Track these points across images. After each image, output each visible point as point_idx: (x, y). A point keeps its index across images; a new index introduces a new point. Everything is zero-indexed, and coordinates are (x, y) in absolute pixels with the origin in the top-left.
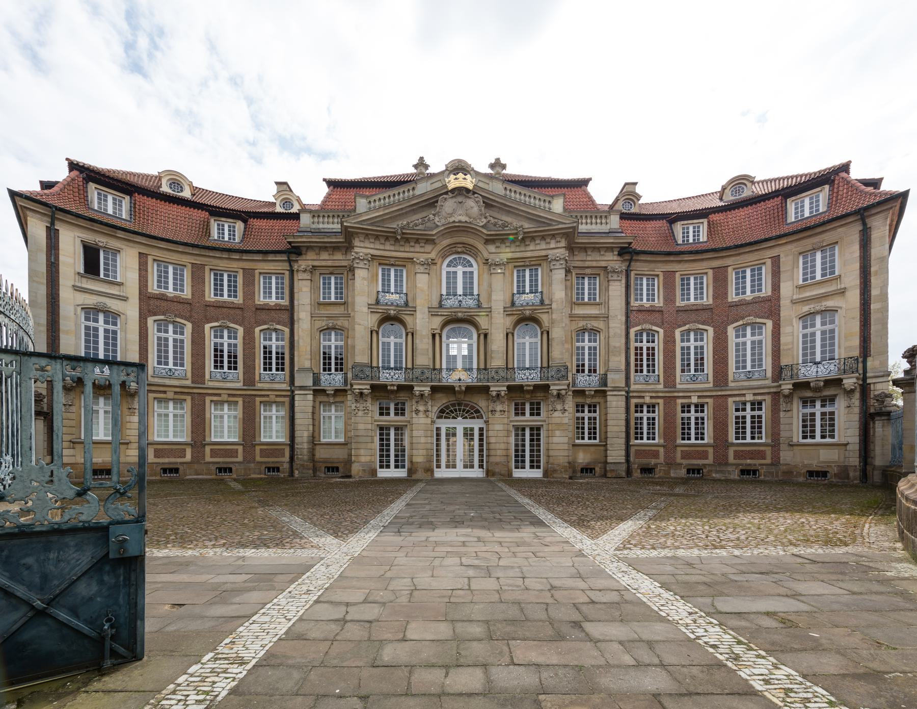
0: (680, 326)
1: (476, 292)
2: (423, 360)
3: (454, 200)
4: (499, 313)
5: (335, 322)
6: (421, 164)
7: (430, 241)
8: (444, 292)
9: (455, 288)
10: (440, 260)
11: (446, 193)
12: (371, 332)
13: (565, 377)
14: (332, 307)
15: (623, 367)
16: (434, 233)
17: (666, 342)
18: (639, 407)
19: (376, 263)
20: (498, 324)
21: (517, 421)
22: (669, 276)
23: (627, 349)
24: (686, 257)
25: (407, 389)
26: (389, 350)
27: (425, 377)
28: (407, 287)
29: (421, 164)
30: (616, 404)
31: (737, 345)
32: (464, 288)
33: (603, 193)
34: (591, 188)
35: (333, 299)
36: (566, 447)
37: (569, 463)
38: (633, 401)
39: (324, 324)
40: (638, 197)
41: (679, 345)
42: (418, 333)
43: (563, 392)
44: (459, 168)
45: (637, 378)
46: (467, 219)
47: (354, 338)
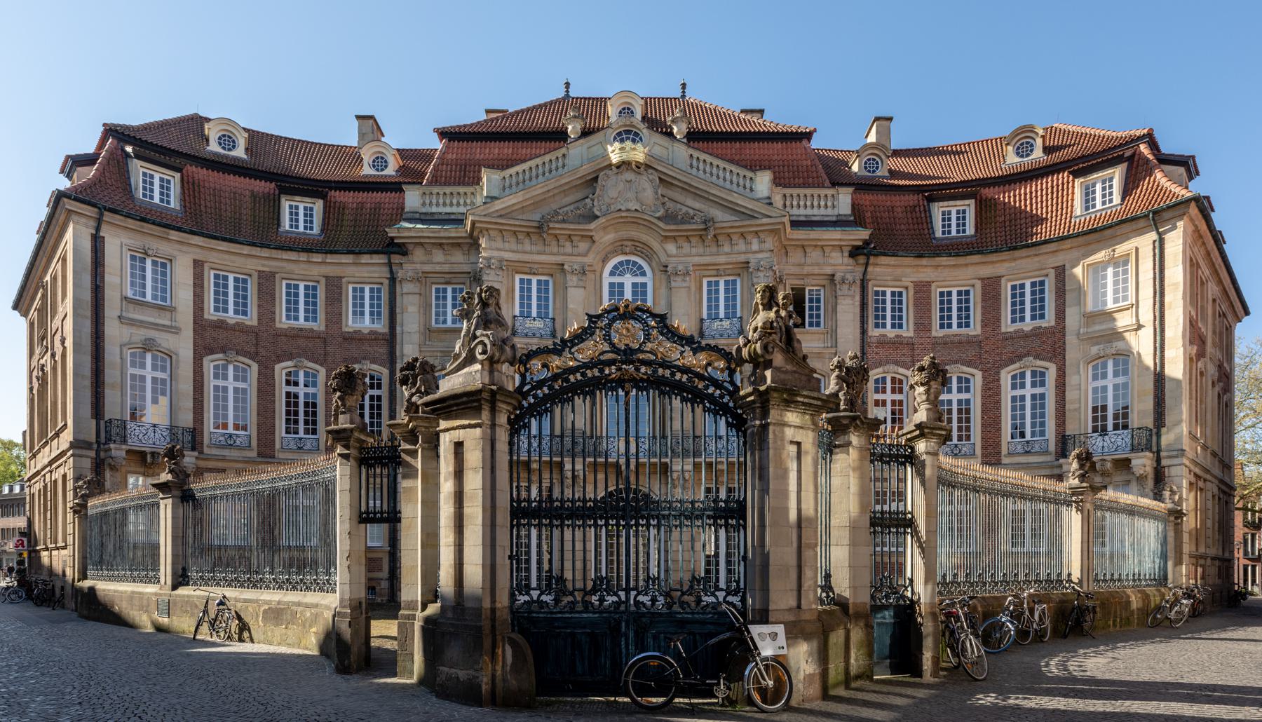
10: (601, 264)
28: (554, 309)
31: (1014, 399)
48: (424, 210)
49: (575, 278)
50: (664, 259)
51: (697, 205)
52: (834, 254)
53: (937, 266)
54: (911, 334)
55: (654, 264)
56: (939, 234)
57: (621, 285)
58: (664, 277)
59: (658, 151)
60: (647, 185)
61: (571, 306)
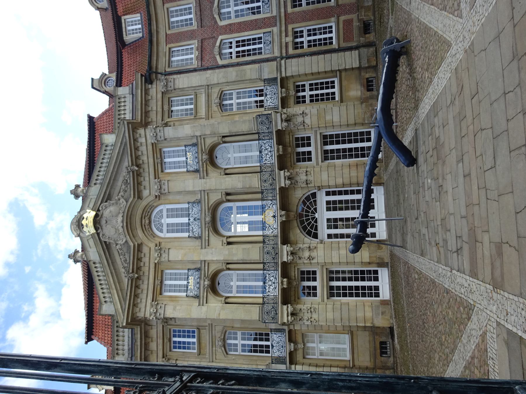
0: (216, 22)
1: (186, 206)
2: (254, 253)
3: (104, 227)
4: (206, 183)
5: (218, 339)
6: (74, 257)
7: (139, 248)
8: (186, 235)
9: (182, 224)
10: (156, 239)
11: (98, 234)
12: (226, 303)
13: (268, 116)
14: (203, 342)
15: (257, 66)
16: (132, 244)
17: (231, 32)
18: (296, 46)
19: (159, 298)
20: (217, 183)
21: (317, 158)
22: (169, 39)
23: (238, 64)
24: (154, 27)
25: (286, 269)
26: (244, 287)
27: (272, 251)
28: (183, 269)
29: (74, 257)
30: (294, 67)
32: (182, 216)
33: (99, 104)
34: (95, 114)
35: (195, 340)
36: (343, 108)
37: (362, 103)
38: (291, 51)
39: (219, 350)
40: (104, 75)
41: (234, 20)
42: (226, 259)
43: (284, 116)
44: (78, 224)
45: (267, 52)
46: (121, 215)
47: (233, 320)
48: (126, 354)
49: (164, 255)
50: (152, 198)
51: (121, 179)
52: (151, 93)
53: (157, 32)
54: (196, 41)
55: (155, 204)
56: (140, 35)
57: (168, 225)
58: (162, 197)
59: (91, 205)
60: (108, 210)
61: (180, 258)
